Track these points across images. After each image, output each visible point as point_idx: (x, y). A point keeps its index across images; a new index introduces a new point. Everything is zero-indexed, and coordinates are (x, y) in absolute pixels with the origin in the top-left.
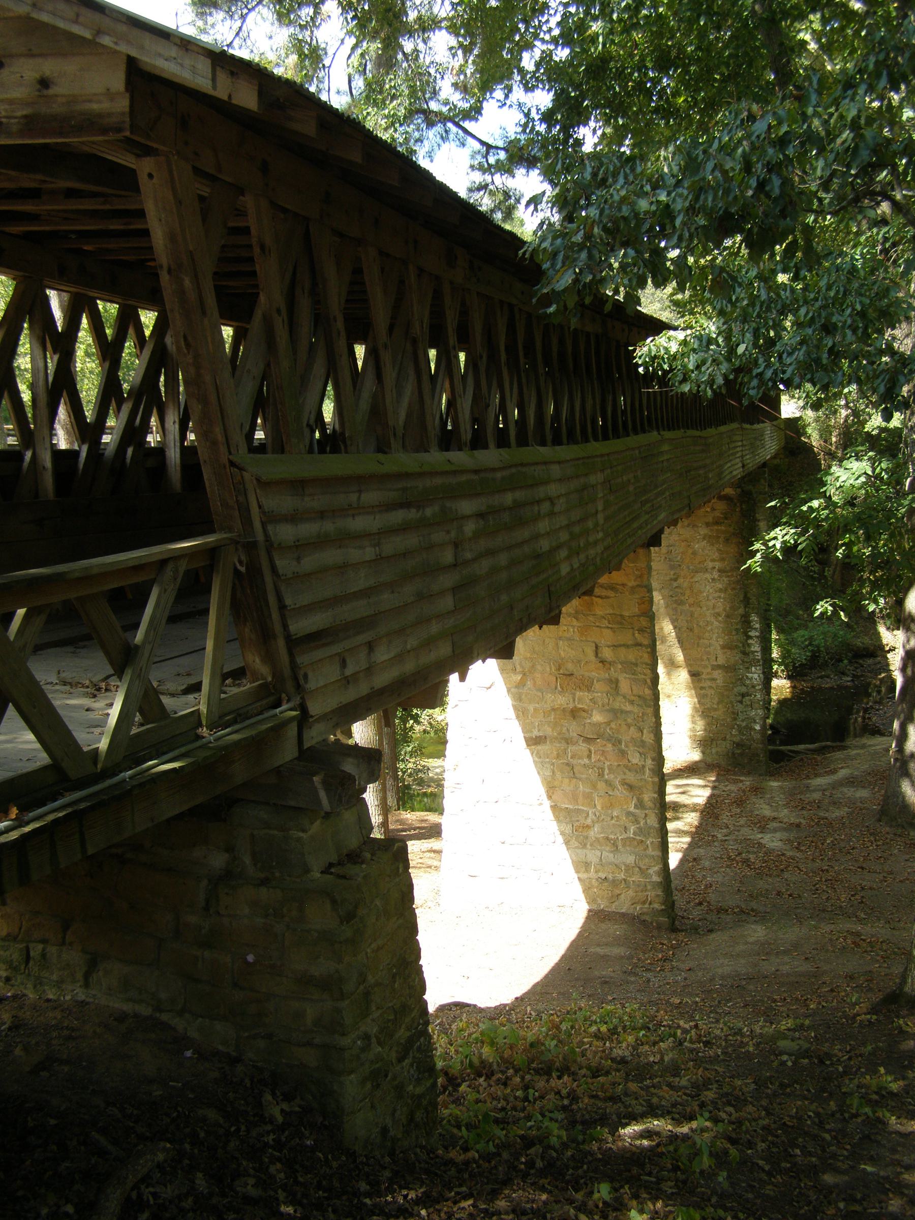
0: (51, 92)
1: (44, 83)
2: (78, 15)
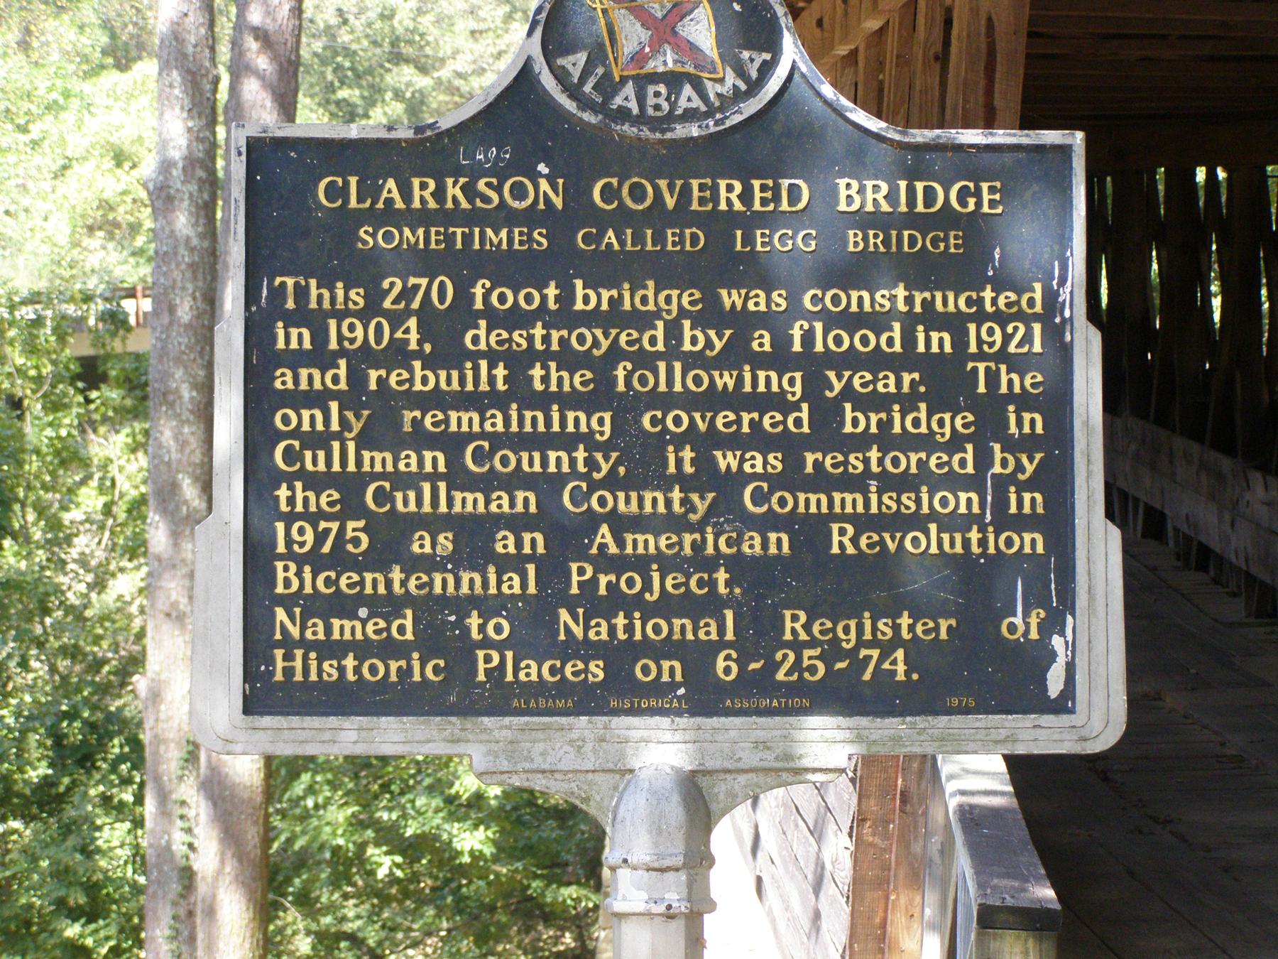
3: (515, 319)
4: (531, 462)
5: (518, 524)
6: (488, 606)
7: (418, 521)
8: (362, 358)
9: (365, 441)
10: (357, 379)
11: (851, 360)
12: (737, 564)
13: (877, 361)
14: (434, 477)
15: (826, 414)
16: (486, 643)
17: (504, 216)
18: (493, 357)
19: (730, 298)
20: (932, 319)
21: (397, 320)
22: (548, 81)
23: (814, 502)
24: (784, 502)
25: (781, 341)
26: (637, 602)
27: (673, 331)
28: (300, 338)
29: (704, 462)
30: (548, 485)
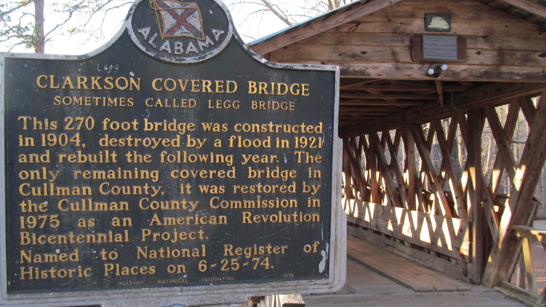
3: (120, 134)
4: (126, 191)
5: (121, 215)
6: (109, 247)
7: (79, 214)
8: (57, 149)
9: (58, 183)
10: (54, 158)
11: (252, 151)
12: (207, 228)
13: (262, 151)
14: (86, 197)
15: (242, 171)
16: (109, 261)
17: (115, 93)
18: (110, 149)
19: (206, 126)
20: (282, 135)
21: (71, 134)
22: (134, 38)
23: (236, 204)
24: (225, 204)
25: (225, 143)
26: (169, 243)
27: (184, 139)
28: (30, 141)
29: (195, 190)
30: (133, 200)
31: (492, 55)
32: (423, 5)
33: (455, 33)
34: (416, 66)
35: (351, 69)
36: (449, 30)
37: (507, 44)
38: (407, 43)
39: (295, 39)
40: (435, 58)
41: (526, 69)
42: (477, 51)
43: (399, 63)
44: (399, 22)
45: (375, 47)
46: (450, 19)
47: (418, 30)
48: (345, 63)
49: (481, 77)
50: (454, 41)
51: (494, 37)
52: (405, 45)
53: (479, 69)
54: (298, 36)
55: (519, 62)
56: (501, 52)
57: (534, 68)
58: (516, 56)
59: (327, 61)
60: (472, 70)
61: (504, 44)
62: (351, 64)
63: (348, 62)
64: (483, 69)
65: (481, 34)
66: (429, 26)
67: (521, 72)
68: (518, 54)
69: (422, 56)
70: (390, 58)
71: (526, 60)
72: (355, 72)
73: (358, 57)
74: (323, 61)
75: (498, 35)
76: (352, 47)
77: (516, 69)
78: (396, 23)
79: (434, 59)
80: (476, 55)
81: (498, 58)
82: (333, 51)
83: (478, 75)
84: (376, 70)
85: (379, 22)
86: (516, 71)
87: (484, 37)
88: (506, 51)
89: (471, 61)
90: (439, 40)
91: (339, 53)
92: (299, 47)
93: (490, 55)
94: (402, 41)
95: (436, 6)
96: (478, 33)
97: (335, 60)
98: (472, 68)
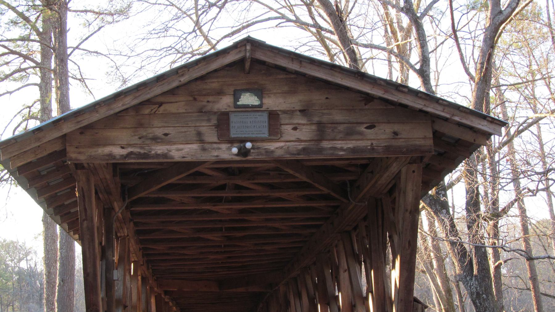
0: (399, 137)
1: (396, 133)
2: (444, 109)
31: (310, 130)
32: (231, 81)
33: (268, 108)
34: (224, 146)
35: (153, 152)
36: (260, 106)
37: (328, 117)
38: (214, 121)
39: (80, 123)
40: (243, 136)
41: (351, 143)
42: (294, 126)
43: (206, 144)
44: (206, 101)
45: (178, 128)
46: (262, 94)
47: (226, 108)
48: (146, 147)
49: (298, 154)
50: (264, 118)
51: (313, 110)
52: (211, 125)
53: (298, 145)
54: (84, 120)
55: (341, 135)
56: (321, 127)
57: (361, 142)
58: (338, 130)
59: (126, 145)
60: (288, 147)
61: (325, 117)
62: (152, 147)
63: (150, 145)
64: (301, 146)
65: (298, 107)
66: (238, 103)
67: (345, 147)
68: (341, 128)
69: (229, 136)
70: (195, 139)
71: (349, 134)
72: (157, 156)
73: (159, 139)
74: (122, 146)
75: (317, 108)
76: (154, 129)
77: (339, 144)
78: (203, 101)
79: (242, 137)
80: (292, 131)
81: (318, 132)
82: (133, 134)
83: (295, 152)
84: (180, 152)
85: (183, 101)
86: (339, 146)
87: (300, 111)
88: (327, 125)
89: (285, 137)
90: (247, 117)
91: (139, 136)
92: (97, 132)
93: (308, 130)
94: (209, 120)
95: (247, 81)
96: (294, 108)
97: (134, 144)
98: (289, 145)
